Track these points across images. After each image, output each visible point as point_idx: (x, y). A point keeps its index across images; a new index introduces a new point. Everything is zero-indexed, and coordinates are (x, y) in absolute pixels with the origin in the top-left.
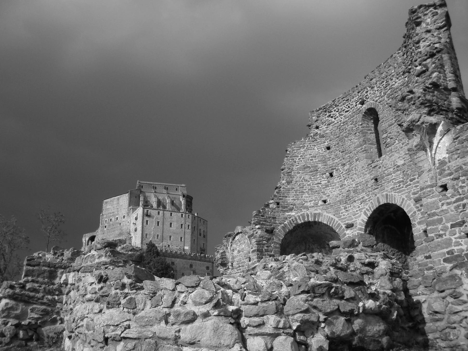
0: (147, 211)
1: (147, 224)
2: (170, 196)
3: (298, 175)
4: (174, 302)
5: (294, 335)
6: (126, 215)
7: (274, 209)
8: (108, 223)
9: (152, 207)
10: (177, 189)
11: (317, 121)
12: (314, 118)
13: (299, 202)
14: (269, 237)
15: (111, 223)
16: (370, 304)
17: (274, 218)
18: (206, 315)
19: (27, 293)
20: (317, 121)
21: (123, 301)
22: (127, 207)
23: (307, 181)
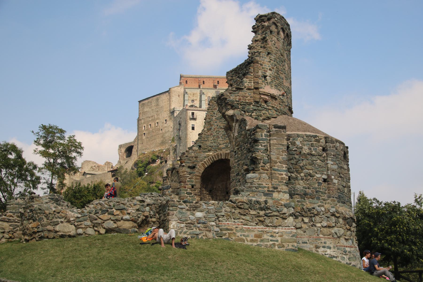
0: (193, 114)
1: (193, 128)
3: (215, 124)
4: (53, 218)
5: (93, 228)
6: (168, 119)
7: (197, 150)
8: (148, 129)
9: (200, 107)
11: (231, 80)
12: (229, 77)
13: (215, 144)
14: (191, 172)
16: (127, 217)
17: (195, 157)
18: (62, 222)
19: (8, 218)
20: (231, 80)
21: (38, 218)
22: (168, 109)
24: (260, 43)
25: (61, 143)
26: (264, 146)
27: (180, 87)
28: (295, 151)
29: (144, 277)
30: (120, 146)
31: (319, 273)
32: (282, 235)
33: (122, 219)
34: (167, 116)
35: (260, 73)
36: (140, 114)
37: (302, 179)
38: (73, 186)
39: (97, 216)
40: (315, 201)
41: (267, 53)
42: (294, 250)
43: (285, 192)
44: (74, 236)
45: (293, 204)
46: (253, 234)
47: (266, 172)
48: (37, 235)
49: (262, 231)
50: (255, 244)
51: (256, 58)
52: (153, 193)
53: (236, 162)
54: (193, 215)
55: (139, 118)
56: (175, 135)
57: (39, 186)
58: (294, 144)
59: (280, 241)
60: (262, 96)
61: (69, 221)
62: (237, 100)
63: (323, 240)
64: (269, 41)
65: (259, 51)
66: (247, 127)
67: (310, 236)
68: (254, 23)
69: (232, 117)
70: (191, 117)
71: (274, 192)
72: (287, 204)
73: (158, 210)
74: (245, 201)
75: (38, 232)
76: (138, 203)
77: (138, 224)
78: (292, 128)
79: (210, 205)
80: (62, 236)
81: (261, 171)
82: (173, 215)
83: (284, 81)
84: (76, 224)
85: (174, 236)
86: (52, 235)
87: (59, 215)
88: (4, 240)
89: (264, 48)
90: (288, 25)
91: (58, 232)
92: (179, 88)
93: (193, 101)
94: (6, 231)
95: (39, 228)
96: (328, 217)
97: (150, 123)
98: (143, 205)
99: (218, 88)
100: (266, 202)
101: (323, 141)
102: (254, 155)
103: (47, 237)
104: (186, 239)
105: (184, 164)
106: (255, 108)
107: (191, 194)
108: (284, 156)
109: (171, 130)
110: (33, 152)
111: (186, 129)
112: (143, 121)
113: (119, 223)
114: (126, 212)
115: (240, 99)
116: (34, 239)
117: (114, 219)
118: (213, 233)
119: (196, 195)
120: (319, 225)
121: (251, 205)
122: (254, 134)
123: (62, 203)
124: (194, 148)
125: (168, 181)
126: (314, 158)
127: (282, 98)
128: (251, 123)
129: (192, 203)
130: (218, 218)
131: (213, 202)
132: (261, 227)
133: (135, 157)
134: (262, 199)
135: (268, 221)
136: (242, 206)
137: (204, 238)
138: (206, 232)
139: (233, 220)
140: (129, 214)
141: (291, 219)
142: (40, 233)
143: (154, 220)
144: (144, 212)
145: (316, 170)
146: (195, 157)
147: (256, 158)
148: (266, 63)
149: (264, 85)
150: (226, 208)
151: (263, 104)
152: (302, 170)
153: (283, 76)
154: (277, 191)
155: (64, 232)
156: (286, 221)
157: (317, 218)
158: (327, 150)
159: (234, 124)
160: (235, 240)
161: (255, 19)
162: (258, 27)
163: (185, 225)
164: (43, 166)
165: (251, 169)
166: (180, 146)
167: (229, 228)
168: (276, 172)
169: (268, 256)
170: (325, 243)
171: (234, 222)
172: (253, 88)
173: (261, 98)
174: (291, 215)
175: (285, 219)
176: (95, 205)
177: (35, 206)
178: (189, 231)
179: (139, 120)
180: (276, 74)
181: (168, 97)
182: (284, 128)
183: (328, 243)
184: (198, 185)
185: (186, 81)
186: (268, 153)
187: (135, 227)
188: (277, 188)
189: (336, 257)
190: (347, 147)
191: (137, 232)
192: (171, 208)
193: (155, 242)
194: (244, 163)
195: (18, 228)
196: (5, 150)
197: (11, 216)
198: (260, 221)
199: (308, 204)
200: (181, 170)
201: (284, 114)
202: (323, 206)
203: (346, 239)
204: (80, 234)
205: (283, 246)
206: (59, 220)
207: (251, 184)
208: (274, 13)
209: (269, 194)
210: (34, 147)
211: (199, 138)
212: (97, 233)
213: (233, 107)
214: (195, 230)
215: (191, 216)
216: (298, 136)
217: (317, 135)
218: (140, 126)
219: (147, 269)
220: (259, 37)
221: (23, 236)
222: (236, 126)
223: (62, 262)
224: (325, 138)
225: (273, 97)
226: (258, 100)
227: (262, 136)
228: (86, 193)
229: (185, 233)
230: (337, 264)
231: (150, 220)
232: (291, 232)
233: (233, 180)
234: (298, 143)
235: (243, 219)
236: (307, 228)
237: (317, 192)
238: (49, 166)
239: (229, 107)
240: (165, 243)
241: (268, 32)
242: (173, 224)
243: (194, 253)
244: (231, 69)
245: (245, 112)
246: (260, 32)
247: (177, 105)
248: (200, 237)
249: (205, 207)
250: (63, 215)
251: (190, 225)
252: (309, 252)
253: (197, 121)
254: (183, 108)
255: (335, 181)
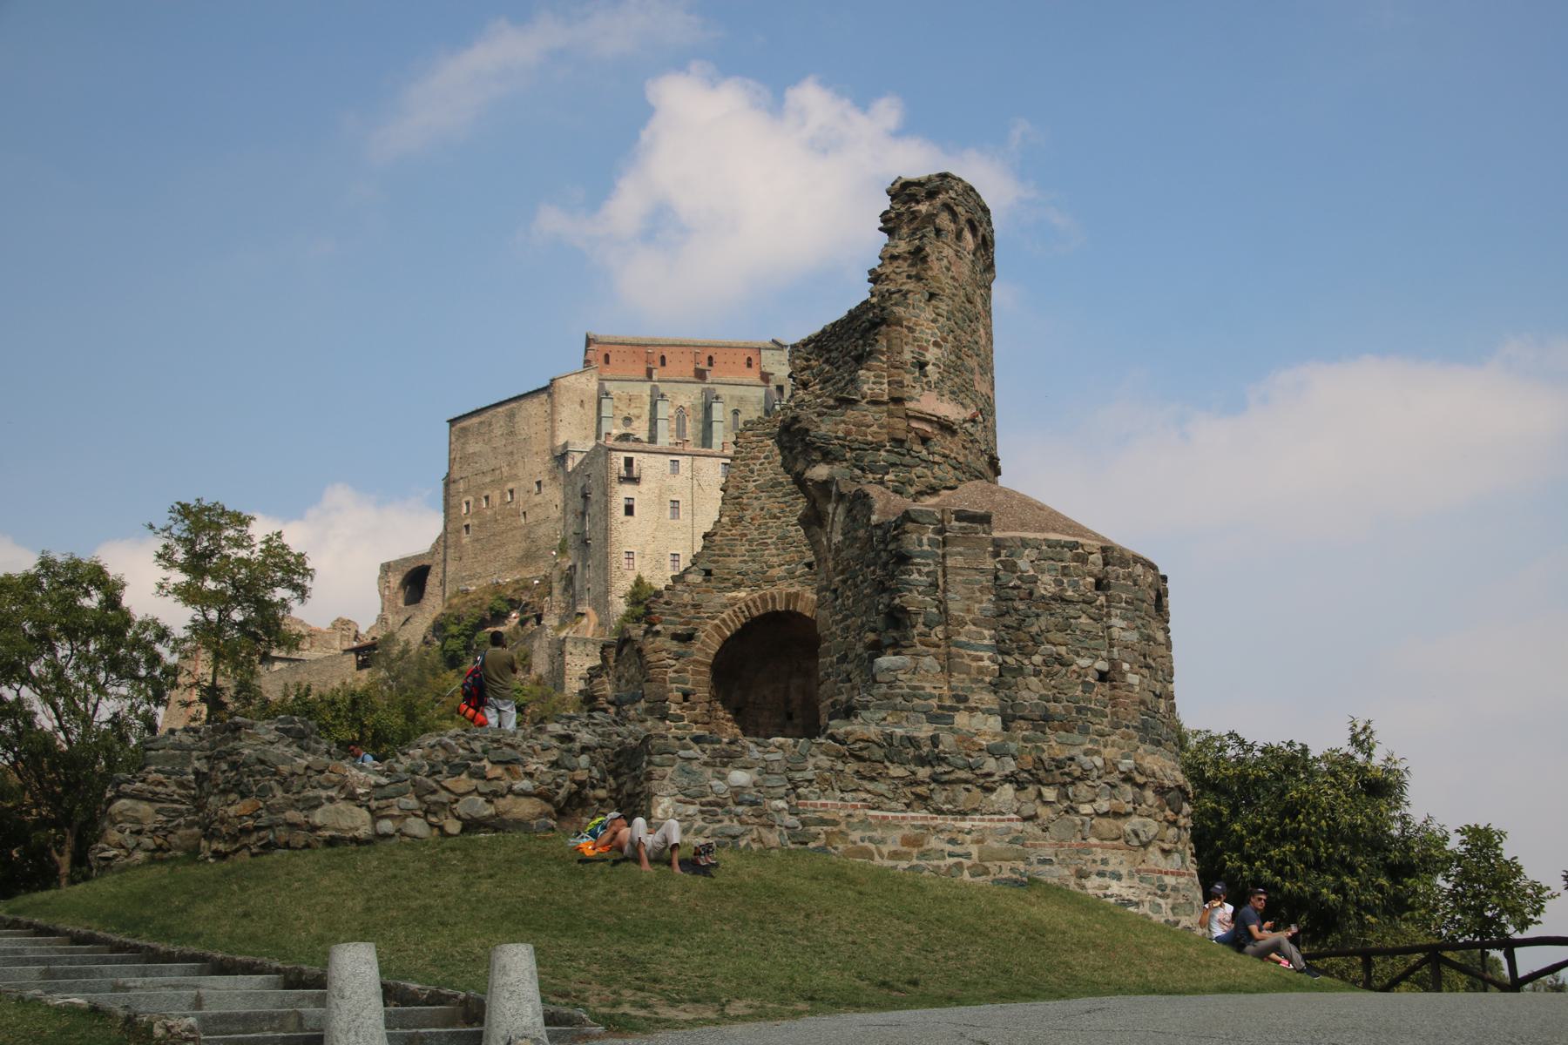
1: (629, 510)
2: (721, 391)
3: (756, 503)
4: (304, 787)
5: (425, 817)
6: (545, 479)
7: (696, 585)
8: (478, 513)
9: (653, 439)
10: (749, 365)
11: (803, 369)
13: (756, 566)
15: (489, 512)
16: (526, 784)
17: (696, 606)
18: (331, 800)
19: (151, 788)
20: (803, 369)
22: (547, 446)
23: (775, 517)
24: (904, 266)
25: (240, 560)
26: (928, 574)
27: (588, 375)
28: (1015, 588)
29: (623, 949)
30: (386, 568)
31: (1095, 946)
32: (981, 837)
33: (510, 790)
34: (542, 468)
35: (907, 356)
36: (451, 462)
37: (1037, 673)
38: (286, 695)
39: (438, 782)
40: (1076, 737)
41: (927, 296)
42: (1016, 881)
43: (990, 712)
44: (367, 842)
45: (1013, 746)
46: (897, 835)
47: (933, 650)
48: (254, 837)
49: (922, 827)
50: (904, 864)
51: (895, 309)
52: (595, 714)
53: (837, 623)
54: (723, 777)
55: (448, 475)
56: (570, 532)
57: (174, 695)
58: (1011, 567)
59: (975, 855)
60: (915, 424)
61: (352, 797)
62: (840, 434)
63: (1099, 854)
64: (932, 258)
65: (905, 288)
66: (874, 518)
67: (1060, 843)
68: (885, 203)
69: (825, 485)
70: (624, 473)
71: (958, 710)
72: (996, 747)
73: (612, 765)
74: (873, 737)
75: (258, 829)
76: (555, 743)
77: (556, 805)
78: (1004, 519)
79: (771, 748)
80: (331, 842)
81: (920, 647)
82: (664, 777)
83: (977, 377)
84: (374, 804)
85: (676, 838)
86: (300, 838)
87: (321, 778)
88: (140, 856)
89: (919, 278)
90: (986, 211)
91: (319, 828)
92: (583, 379)
93: (628, 420)
94: (147, 828)
95: (259, 816)
96: (1113, 786)
97: (486, 492)
98: (569, 751)
99: (709, 380)
100: (935, 740)
101: (1096, 558)
102: (897, 601)
103: (287, 845)
104: (707, 849)
105: (658, 627)
106: (894, 458)
107: (681, 718)
108: (986, 603)
109: (557, 514)
110: (155, 588)
111: (606, 511)
112: (462, 486)
113: (502, 804)
114: (521, 769)
115: (848, 433)
116: (245, 852)
117: (486, 790)
118: (781, 833)
119: (696, 722)
120: (1086, 809)
121: (893, 749)
122: (896, 538)
123: (312, 744)
124: (690, 578)
125: (605, 679)
126: (1071, 611)
127: (972, 430)
128: (885, 504)
129: (719, 742)
130: (795, 787)
131: (781, 739)
132: (920, 815)
133: (434, 605)
134: (925, 731)
135: (940, 797)
136: (865, 754)
137: (755, 846)
138: (762, 830)
139: (838, 793)
140: (530, 775)
141: (1008, 790)
142: (262, 834)
143: (602, 793)
144: (573, 770)
145: (1077, 647)
146: (694, 606)
147: (903, 610)
148: (924, 324)
149: (918, 390)
150: (818, 760)
151: (917, 447)
152: (1037, 644)
153: (972, 363)
154: (966, 709)
155: (336, 830)
156: (993, 797)
157: (1082, 789)
158: (1108, 587)
159: (830, 509)
160: (848, 854)
161: (888, 192)
162: (899, 215)
163: (698, 807)
164: (188, 633)
165: (887, 642)
166: (584, 566)
167: (826, 816)
168: (962, 651)
169: (947, 900)
170: (1105, 862)
171: (842, 799)
172: (886, 398)
173: (910, 429)
174: (1008, 779)
175: (989, 790)
176: (427, 750)
177: (246, 752)
178: (711, 826)
179: (449, 482)
180: (953, 358)
181: (548, 407)
182: (985, 519)
183: (1112, 861)
184: (703, 693)
185: (607, 356)
186: (939, 594)
187: (549, 815)
188: (966, 699)
189: (1137, 904)
190: (1164, 578)
191: (553, 829)
192: (657, 759)
193: (619, 856)
194: (863, 625)
195: (182, 820)
196: (70, 583)
197: (160, 783)
198: (918, 796)
199: (1054, 746)
200: (651, 644)
201: (977, 477)
202: (1098, 753)
203: (1164, 851)
204: (386, 836)
205: (986, 872)
206: (324, 794)
207: (890, 687)
208: (944, 176)
209: (941, 716)
210: (159, 573)
211: (704, 547)
212: (436, 831)
213: (828, 457)
214: (727, 822)
215: (715, 782)
216: (1025, 543)
217: (1081, 540)
218: (453, 501)
219: (621, 929)
220: (903, 247)
221: (204, 843)
222: (837, 514)
223: (368, 910)
224: (1104, 550)
225: (946, 427)
226: (900, 435)
227: (920, 544)
228: (328, 718)
229: (699, 832)
230: (1143, 923)
231: (591, 793)
232: (1008, 831)
233: (828, 675)
234: (1023, 564)
235: (869, 792)
236: (1053, 817)
237: (1079, 710)
238: (204, 631)
239: (816, 456)
240: (650, 861)
241: (930, 229)
242: (663, 805)
243: (740, 887)
244: (805, 336)
245: (863, 470)
246: (905, 231)
247: (575, 434)
248: (743, 843)
249: (757, 755)
250: (333, 777)
251: (713, 808)
252: (1058, 888)
253: (643, 486)
254: (598, 445)
255: (1133, 679)
